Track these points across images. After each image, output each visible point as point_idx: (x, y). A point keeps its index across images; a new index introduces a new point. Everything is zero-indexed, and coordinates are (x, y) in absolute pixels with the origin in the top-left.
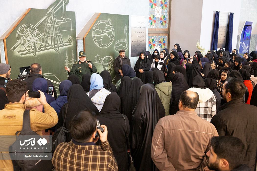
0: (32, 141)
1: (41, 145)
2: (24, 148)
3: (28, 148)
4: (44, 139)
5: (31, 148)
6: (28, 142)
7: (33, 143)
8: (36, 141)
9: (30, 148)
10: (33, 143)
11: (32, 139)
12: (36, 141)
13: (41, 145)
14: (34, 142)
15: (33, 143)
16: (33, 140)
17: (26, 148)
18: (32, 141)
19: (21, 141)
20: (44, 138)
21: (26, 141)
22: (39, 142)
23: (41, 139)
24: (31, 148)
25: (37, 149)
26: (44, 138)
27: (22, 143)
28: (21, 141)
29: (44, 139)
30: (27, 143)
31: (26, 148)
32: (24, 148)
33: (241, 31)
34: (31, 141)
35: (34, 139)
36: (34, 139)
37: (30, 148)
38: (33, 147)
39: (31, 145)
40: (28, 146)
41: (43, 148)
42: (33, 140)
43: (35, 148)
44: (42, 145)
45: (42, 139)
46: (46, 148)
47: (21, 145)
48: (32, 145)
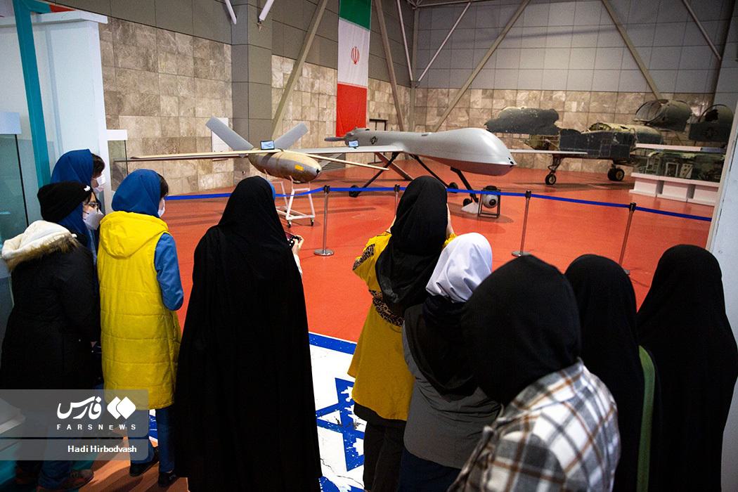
0: (92, 404)
1: (117, 416)
2: (69, 427)
3: (80, 427)
4: (126, 399)
5: (90, 427)
6: (81, 409)
7: (95, 410)
8: (104, 405)
9: (85, 427)
10: (94, 413)
11: (92, 399)
12: (104, 405)
13: (117, 416)
14: (98, 408)
15: (94, 413)
16: (95, 402)
17: (74, 427)
18: (92, 404)
19: (60, 404)
20: (126, 398)
21: (74, 405)
22: (111, 408)
23: (116, 400)
24: (90, 427)
25: (106, 427)
26: (126, 398)
27: (63, 411)
28: (60, 404)
29: (126, 399)
30: (77, 411)
31: (74, 427)
32: (69, 427)
33: (402, 46)
34: (88, 405)
35: (99, 399)
36: (99, 399)
37: (85, 427)
38: (95, 423)
39: (88, 417)
40: (79, 421)
41: (122, 427)
42: (95, 402)
43: (101, 427)
44: (121, 416)
45: (121, 399)
46: (133, 427)
47: (61, 416)
48: (92, 417)
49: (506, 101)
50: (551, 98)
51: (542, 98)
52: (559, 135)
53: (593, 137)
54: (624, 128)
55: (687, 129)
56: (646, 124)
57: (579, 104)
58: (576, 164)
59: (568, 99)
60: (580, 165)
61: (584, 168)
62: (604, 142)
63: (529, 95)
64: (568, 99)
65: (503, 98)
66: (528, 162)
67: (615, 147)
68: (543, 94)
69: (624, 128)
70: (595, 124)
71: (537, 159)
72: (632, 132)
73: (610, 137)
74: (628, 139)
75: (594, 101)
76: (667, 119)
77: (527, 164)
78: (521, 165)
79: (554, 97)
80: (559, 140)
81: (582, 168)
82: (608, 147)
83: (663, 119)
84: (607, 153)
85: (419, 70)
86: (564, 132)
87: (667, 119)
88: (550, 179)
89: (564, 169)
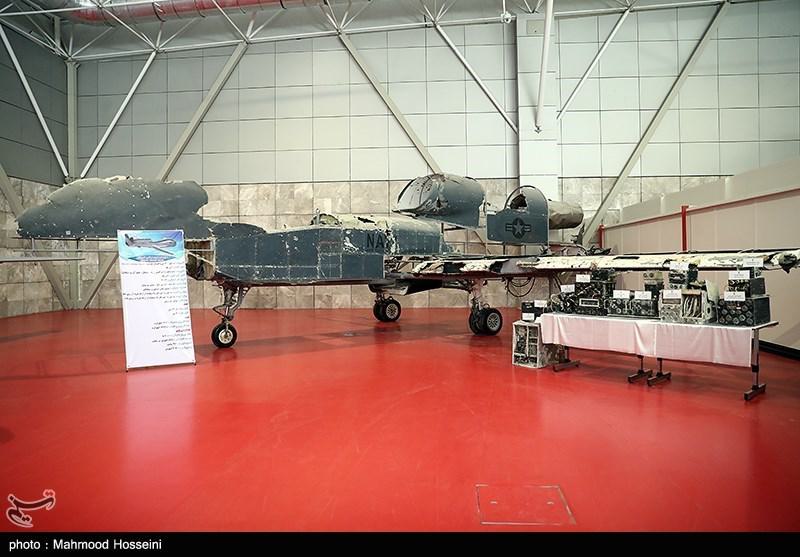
49: (224, 203)
50: (292, 195)
51: (278, 195)
52: (213, 239)
53: (296, 239)
54: (366, 221)
55: (483, 221)
56: (417, 213)
57: (334, 201)
58: (343, 296)
59: (318, 194)
60: (349, 296)
61: (355, 301)
62: (325, 248)
63: (257, 190)
64: (318, 194)
65: (219, 199)
66: (268, 298)
67: (351, 260)
68: (279, 191)
69: (366, 221)
70: (315, 218)
71: (281, 292)
72: (384, 229)
73: (337, 239)
74: (374, 241)
75: (355, 197)
76: (444, 205)
77: (267, 302)
78: (257, 304)
79: (295, 192)
80: (213, 247)
81: (352, 302)
82: (335, 259)
83: (439, 205)
84: (335, 271)
85: (82, 158)
86: (222, 230)
87: (444, 205)
88: (222, 334)
89: (324, 306)
